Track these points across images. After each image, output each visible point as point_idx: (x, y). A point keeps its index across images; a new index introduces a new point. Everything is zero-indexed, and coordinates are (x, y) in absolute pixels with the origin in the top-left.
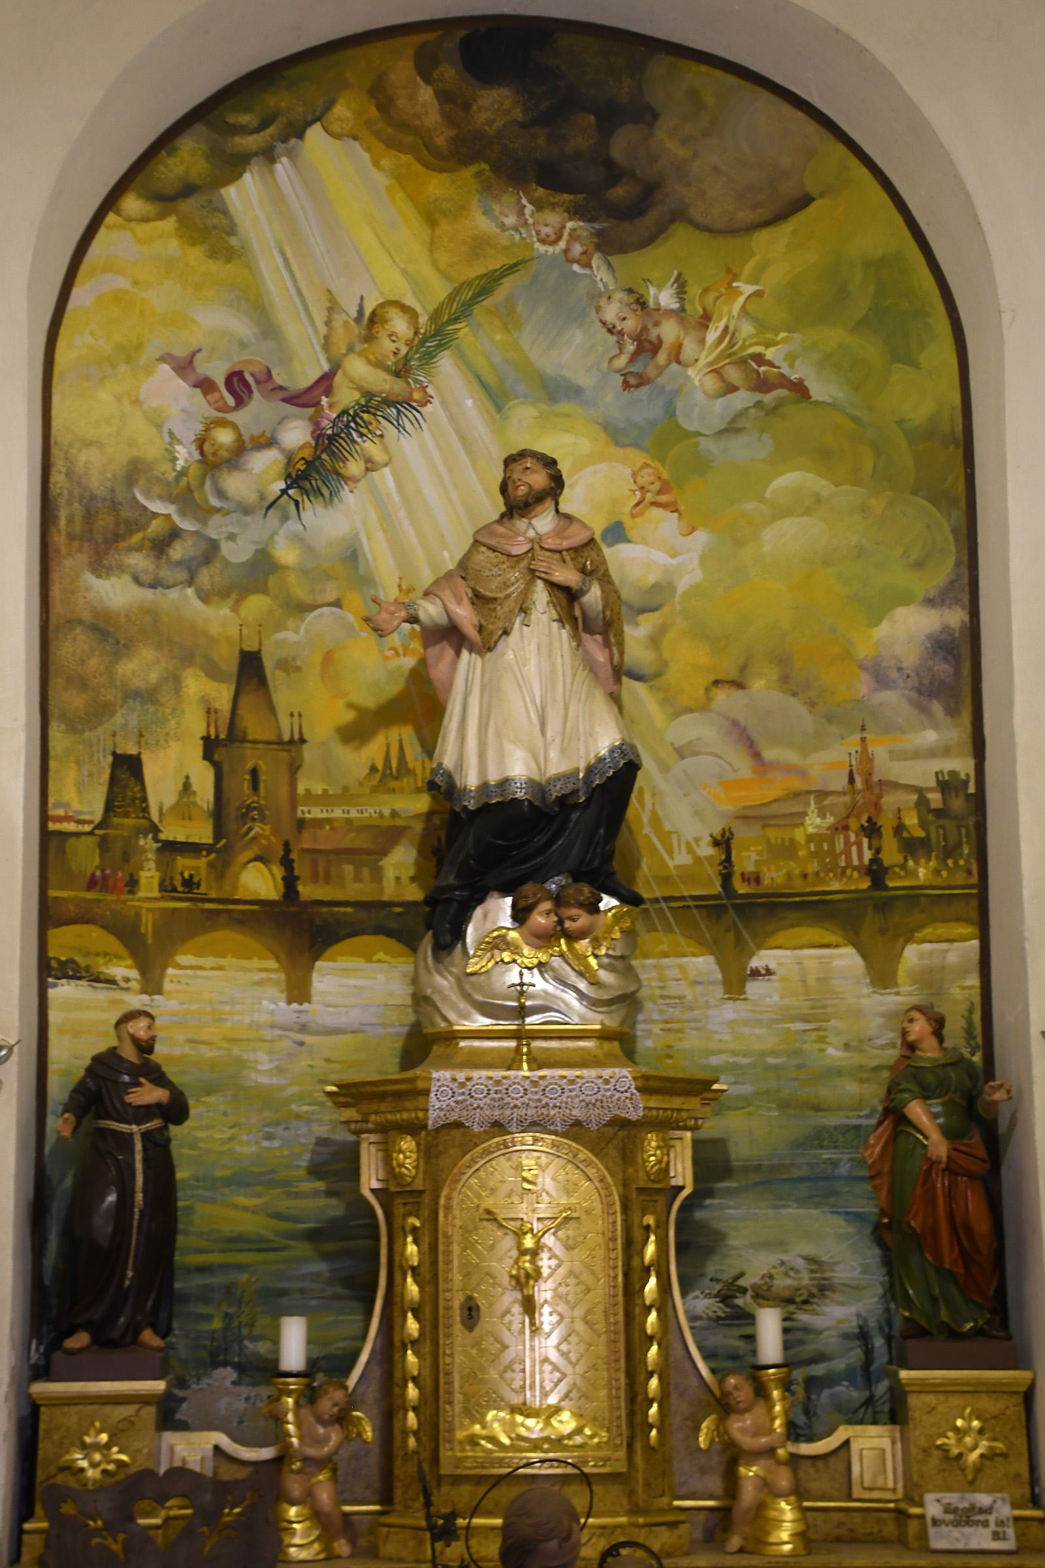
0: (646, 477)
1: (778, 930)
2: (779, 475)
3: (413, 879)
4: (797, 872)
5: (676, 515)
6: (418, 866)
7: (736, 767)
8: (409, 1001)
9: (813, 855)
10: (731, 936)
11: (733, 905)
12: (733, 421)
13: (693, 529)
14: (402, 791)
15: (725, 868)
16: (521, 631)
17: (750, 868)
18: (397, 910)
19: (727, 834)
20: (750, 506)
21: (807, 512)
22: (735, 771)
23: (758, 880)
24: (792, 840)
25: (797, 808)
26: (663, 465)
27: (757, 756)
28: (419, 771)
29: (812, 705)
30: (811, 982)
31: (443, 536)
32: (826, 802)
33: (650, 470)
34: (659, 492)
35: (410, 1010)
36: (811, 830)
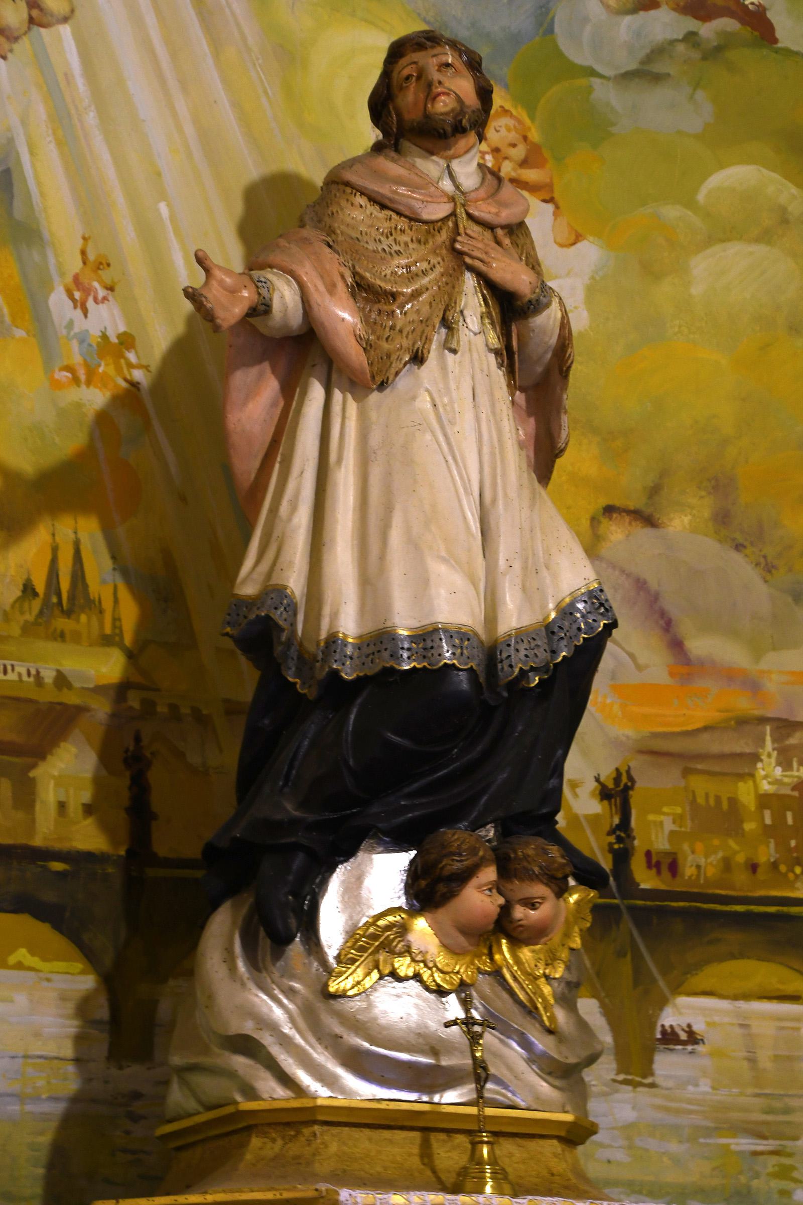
0: (503, 131)
1: (708, 962)
2: (721, 166)
3: (88, 810)
4: (740, 858)
5: (550, 207)
6: (97, 781)
7: (642, 661)
8: (68, 1051)
9: (768, 831)
10: (626, 967)
11: (632, 909)
12: (649, 59)
13: (578, 238)
14: (77, 638)
15: (619, 840)
16: (442, 358)
17: (661, 844)
18: (57, 866)
19: (624, 779)
20: (672, 212)
21: (765, 237)
22: (639, 667)
23: (674, 868)
24: (733, 802)
25: (742, 746)
26: (532, 118)
27: (677, 645)
28: (107, 604)
29: (768, 568)
30: (765, 1061)
31: (159, 174)
32: (792, 741)
33: (510, 122)
34: (524, 163)
35: (71, 1068)
36: (766, 787)
